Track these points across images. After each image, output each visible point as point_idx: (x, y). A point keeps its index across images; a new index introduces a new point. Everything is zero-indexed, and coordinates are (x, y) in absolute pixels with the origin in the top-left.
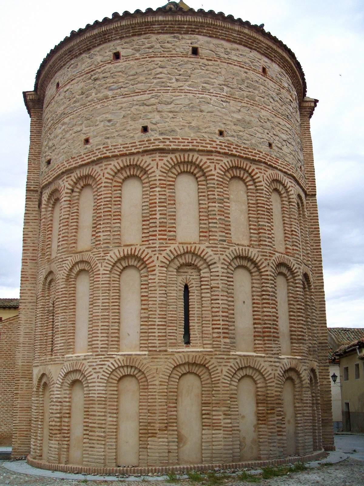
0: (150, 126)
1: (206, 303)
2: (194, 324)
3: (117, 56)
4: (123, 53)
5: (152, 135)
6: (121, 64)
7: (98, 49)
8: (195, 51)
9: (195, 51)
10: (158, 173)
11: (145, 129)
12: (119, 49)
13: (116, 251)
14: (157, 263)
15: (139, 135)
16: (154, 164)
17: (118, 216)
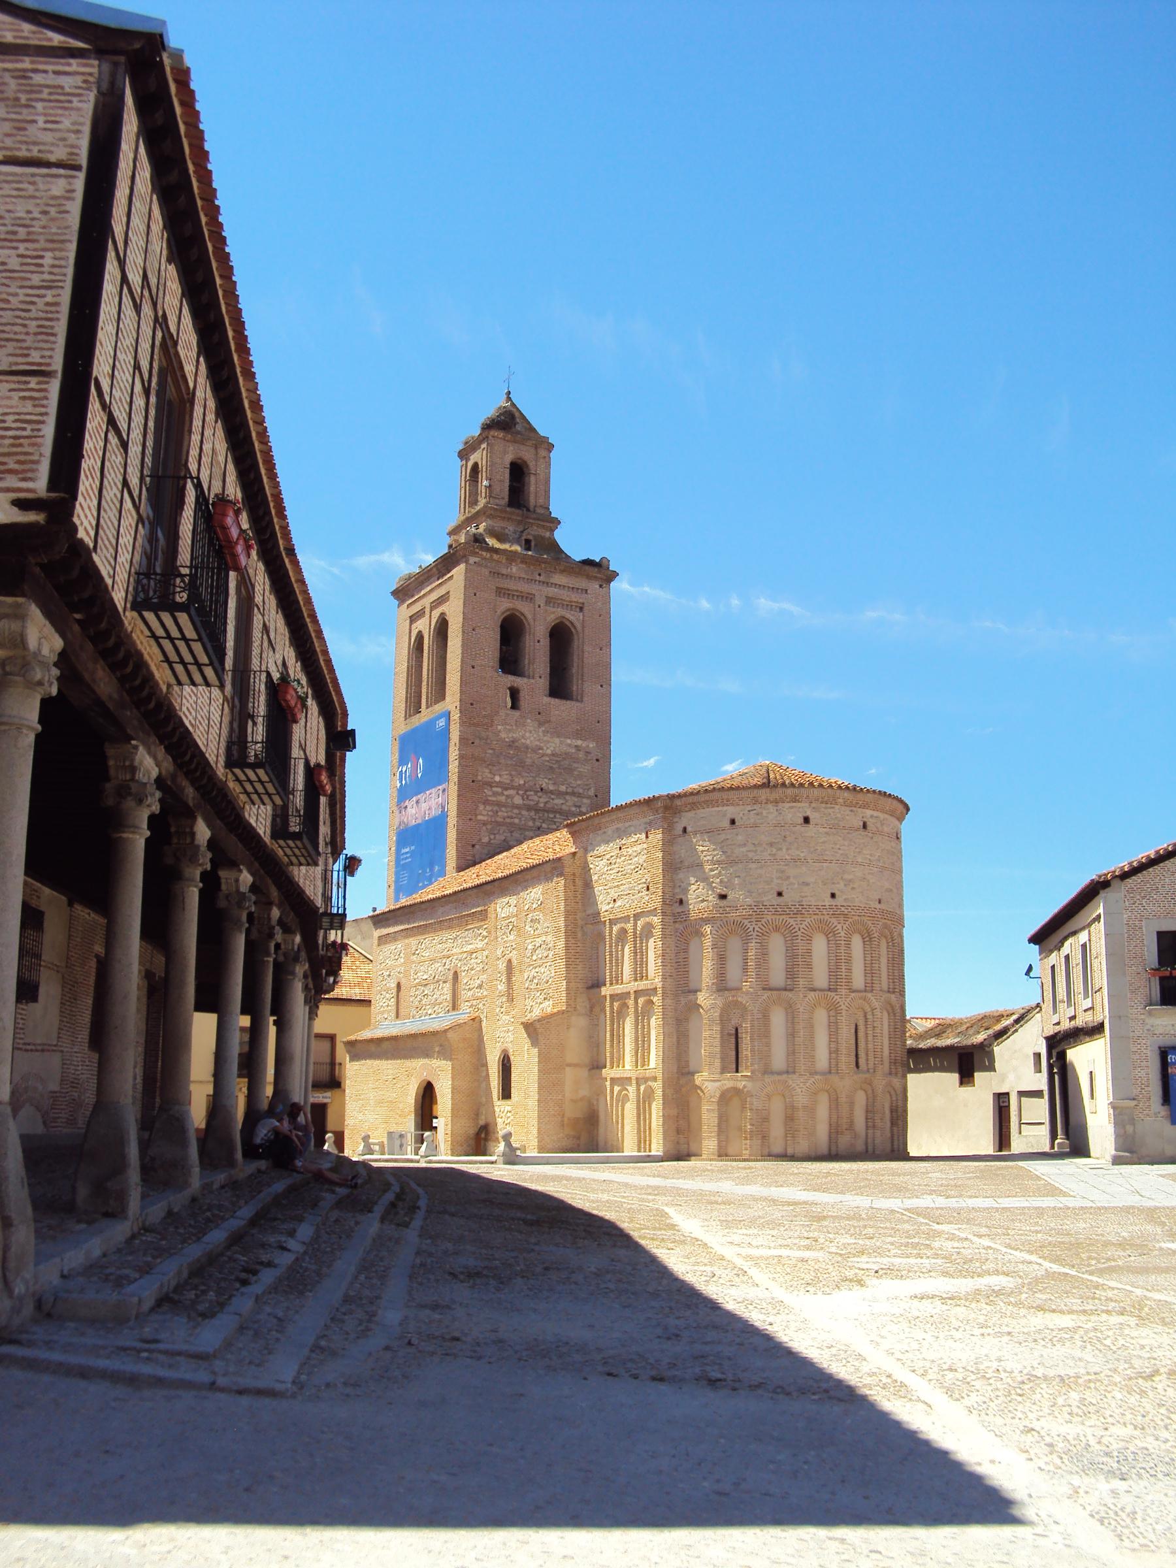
0: (837, 893)
1: (870, 1038)
2: (862, 1054)
3: (806, 820)
4: (811, 818)
5: (839, 901)
6: (810, 830)
7: (787, 805)
8: (865, 826)
9: (865, 826)
10: (842, 934)
11: (833, 896)
12: (808, 813)
13: (812, 994)
14: (843, 1007)
15: (828, 901)
16: (839, 926)
17: (809, 966)
